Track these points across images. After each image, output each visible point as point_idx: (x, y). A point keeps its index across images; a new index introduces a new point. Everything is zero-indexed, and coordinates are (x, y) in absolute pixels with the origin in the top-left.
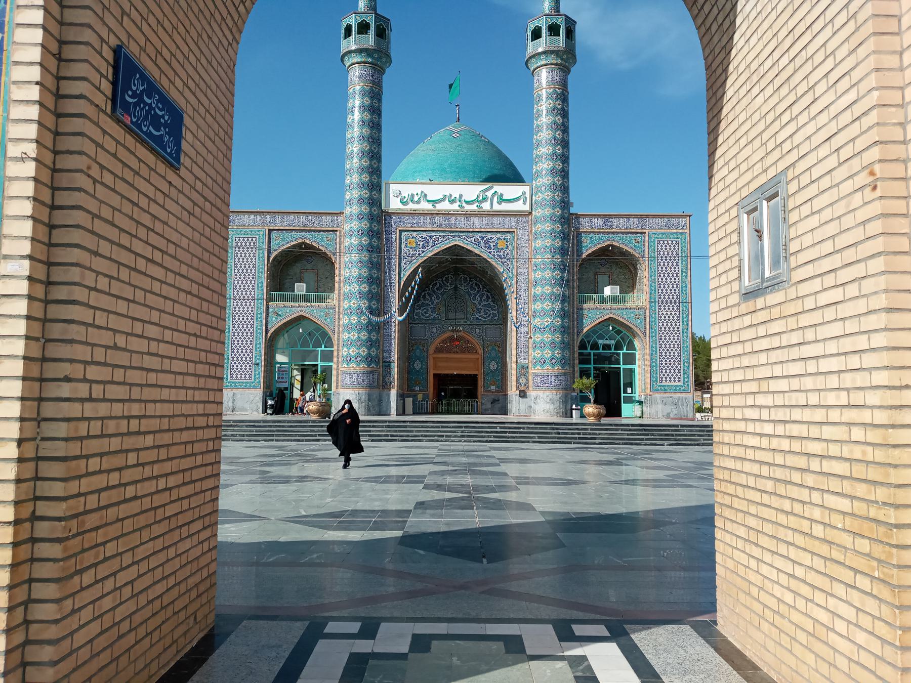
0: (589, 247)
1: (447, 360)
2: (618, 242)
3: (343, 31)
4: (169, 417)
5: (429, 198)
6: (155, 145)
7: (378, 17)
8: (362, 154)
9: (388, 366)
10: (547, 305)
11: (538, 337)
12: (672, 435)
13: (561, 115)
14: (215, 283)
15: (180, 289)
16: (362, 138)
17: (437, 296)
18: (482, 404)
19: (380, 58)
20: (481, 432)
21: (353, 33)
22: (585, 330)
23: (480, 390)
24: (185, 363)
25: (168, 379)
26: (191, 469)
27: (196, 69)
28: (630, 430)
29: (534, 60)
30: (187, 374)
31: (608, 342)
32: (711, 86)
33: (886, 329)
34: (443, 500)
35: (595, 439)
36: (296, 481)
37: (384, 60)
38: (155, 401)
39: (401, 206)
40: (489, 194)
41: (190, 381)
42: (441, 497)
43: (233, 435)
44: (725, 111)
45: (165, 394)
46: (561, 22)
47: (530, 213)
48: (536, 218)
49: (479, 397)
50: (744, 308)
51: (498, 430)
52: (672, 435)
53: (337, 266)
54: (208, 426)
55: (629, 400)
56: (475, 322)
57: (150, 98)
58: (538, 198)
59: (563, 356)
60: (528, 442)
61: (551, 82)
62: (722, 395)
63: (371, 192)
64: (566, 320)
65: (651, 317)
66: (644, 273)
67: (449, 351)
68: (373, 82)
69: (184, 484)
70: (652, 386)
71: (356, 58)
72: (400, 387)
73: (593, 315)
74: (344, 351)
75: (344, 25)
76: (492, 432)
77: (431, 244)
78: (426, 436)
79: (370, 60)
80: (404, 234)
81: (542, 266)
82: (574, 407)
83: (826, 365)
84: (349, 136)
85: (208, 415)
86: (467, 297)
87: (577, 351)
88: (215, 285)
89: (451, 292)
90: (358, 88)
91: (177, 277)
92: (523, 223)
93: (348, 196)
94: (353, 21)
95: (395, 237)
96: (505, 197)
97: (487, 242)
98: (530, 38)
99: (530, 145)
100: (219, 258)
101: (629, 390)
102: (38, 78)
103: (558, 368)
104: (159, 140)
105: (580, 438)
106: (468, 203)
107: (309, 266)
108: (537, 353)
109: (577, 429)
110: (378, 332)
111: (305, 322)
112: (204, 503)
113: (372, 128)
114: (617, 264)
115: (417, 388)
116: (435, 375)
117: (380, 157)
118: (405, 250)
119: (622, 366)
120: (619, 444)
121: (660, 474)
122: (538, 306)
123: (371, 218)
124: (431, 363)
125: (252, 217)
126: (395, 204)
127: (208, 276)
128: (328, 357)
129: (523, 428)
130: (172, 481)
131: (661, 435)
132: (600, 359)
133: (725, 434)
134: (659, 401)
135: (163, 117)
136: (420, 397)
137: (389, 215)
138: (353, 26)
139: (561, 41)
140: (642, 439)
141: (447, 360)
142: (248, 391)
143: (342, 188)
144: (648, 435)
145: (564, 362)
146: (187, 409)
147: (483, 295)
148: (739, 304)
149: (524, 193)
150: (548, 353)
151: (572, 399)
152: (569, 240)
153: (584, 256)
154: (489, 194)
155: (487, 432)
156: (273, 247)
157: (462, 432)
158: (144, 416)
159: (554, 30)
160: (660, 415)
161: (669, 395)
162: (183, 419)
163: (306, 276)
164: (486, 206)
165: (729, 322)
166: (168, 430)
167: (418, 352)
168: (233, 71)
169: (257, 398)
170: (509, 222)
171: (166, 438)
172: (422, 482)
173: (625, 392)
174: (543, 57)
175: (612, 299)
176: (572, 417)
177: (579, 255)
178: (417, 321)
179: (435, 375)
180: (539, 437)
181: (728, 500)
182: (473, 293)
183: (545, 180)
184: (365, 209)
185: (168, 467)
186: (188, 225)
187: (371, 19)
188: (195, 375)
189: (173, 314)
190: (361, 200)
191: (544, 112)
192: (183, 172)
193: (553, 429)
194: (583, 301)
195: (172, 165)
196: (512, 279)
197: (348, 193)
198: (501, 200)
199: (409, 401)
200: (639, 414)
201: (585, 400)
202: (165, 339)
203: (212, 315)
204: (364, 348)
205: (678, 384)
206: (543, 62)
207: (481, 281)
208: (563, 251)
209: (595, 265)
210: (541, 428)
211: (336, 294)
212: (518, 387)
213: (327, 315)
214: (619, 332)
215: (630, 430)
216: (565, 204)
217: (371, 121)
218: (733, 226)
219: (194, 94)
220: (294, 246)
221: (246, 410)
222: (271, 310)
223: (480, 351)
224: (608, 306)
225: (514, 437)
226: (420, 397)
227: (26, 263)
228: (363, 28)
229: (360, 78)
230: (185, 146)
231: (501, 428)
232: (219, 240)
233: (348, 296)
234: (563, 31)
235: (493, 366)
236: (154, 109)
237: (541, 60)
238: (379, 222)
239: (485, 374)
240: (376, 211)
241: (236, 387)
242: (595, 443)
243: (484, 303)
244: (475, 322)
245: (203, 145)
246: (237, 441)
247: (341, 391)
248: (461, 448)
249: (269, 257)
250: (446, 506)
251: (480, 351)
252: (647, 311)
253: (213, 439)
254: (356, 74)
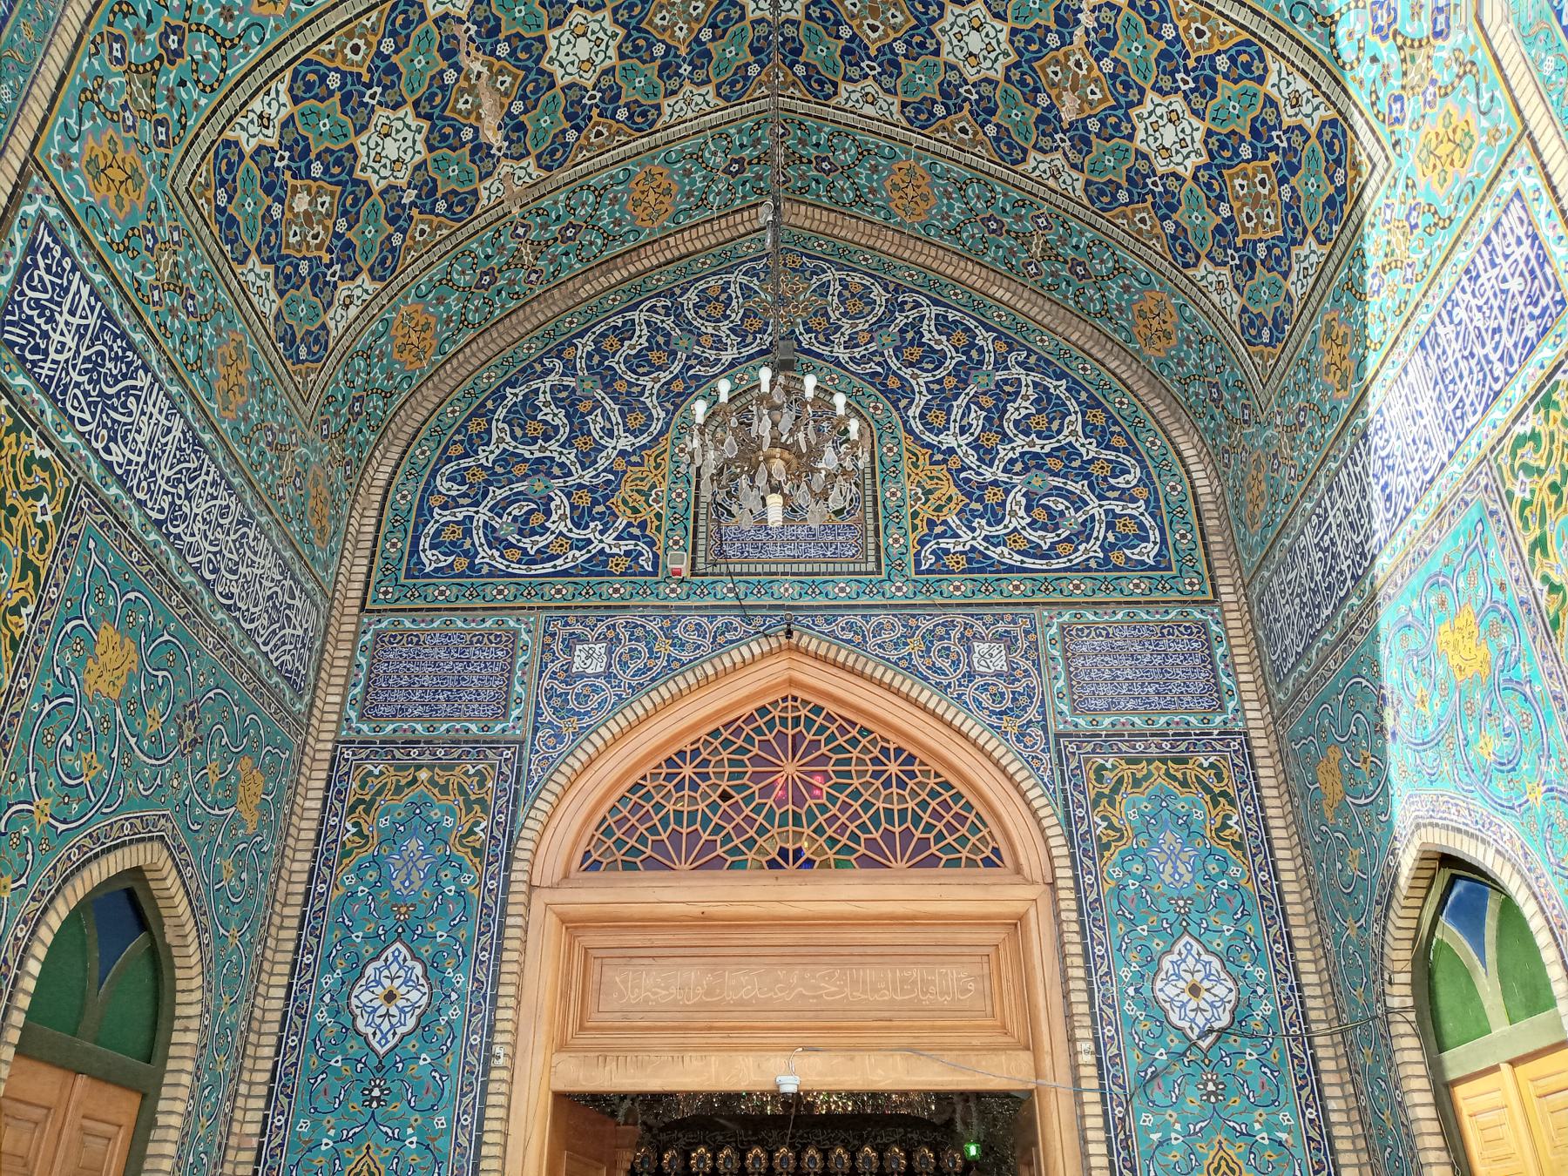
1: (712, 934)
17: (630, 403)
56: (957, 587)
124: (536, 966)
141: (712, 934)
147: (1004, 394)
182: (920, 381)
207: (978, 304)
239: (1121, 1094)
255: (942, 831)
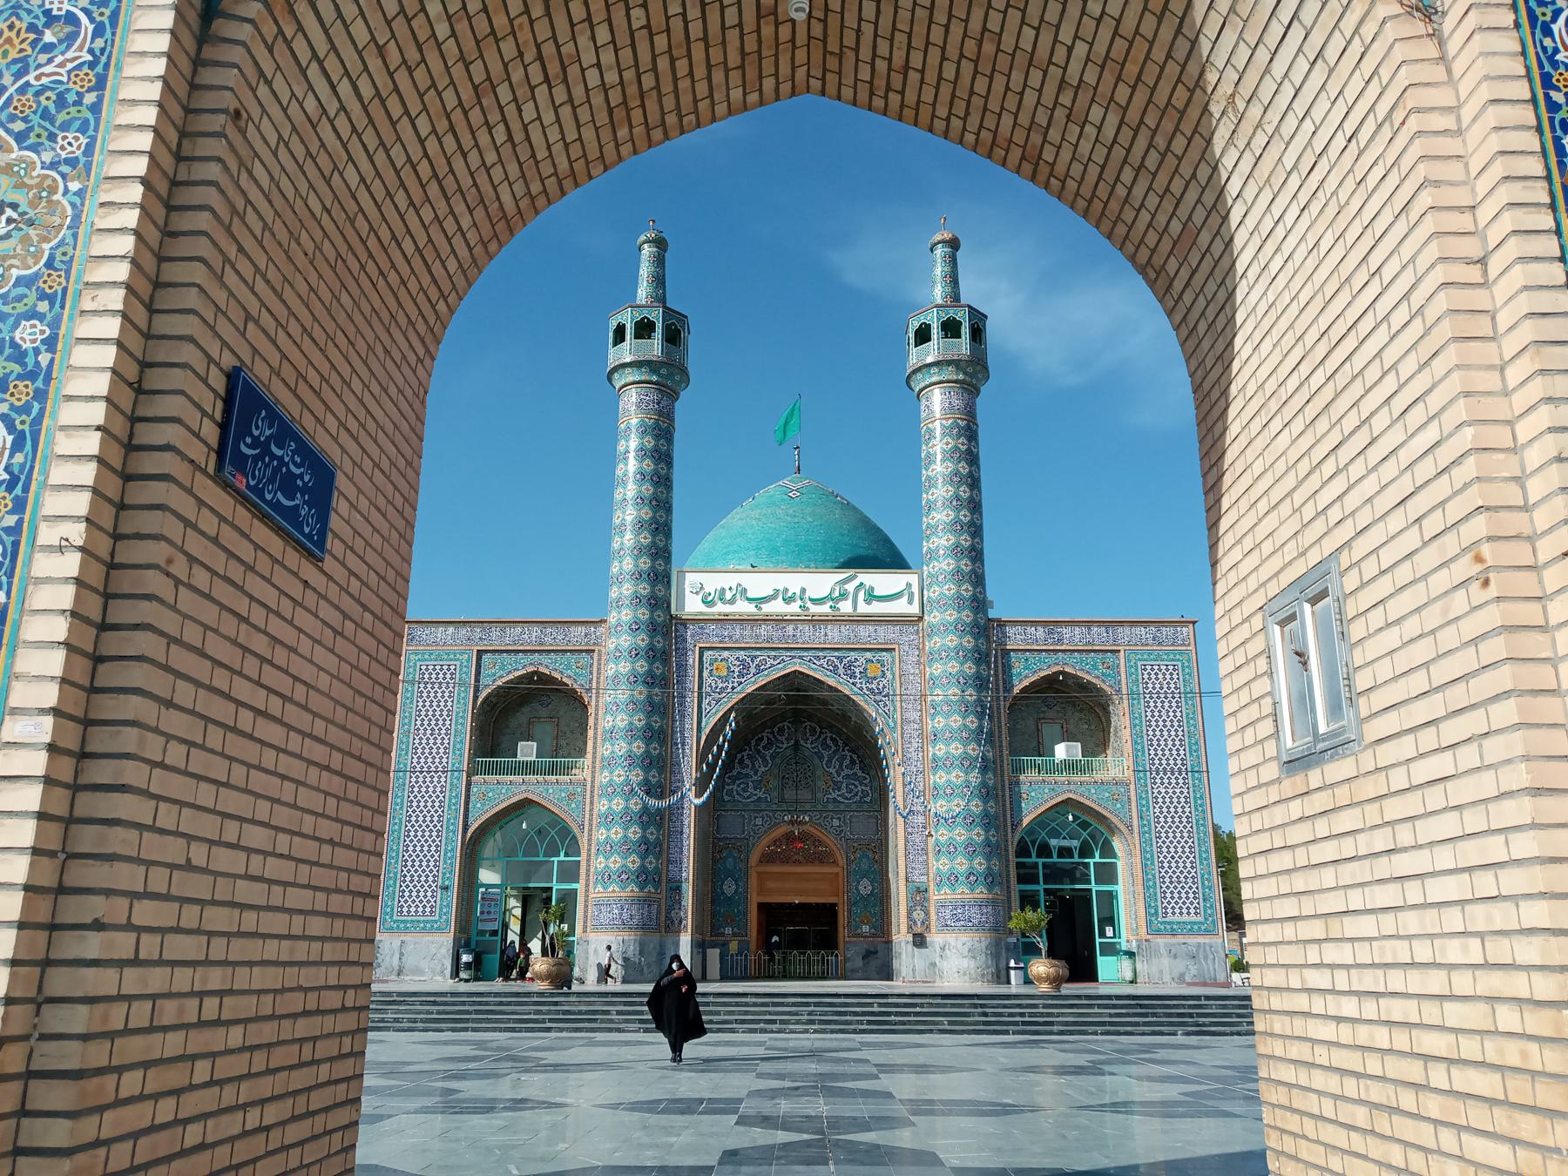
0: (1024, 675)
2: (1073, 666)
3: (611, 334)
4: (275, 991)
5: (750, 595)
6: (285, 522)
7: (668, 312)
8: (640, 525)
9: (676, 889)
10: (957, 777)
11: (942, 835)
12: (1191, 1015)
13: (966, 460)
14: (373, 749)
15: (310, 762)
16: (641, 500)
17: (764, 760)
18: (846, 960)
19: (670, 376)
20: (845, 1014)
21: (628, 337)
22: (1026, 821)
23: (843, 933)
24: (311, 892)
25: (276, 923)
26: (309, 1089)
27: (361, 401)
28: (1115, 1006)
29: (919, 376)
30: (313, 912)
31: (1065, 843)
32: (1204, 418)
33: (1534, 826)
34: (773, 1147)
35: (1052, 1024)
36: (505, 1109)
37: (677, 378)
38: (251, 964)
39: (703, 608)
40: (851, 587)
41: (317, 926)
42: (770, 1142)
43: (396, 1020)
44: (1229, 457)
45: (271, 950)
46: (962, 316)
47: (921, 618)
48: (931, 626)
49: (841, 945)
50: (1290, 786)
51: (876, 1009)
52: (1191, 1015)
53: (591, 710)
54: (344, 1009)
55: (1111, 950)
57: (281, 447)
58: (932, 593)
59: (989, 868)
60: (931, 1031)
61: (949, 410)
62: (1265, 944)
63: (653, 587)
64: (991, 803)
65: (1139, 798)
66: (1121, 720)
67: (785, 859)
68: (660, 413)
69: (294, 1118)
70: (1149, 924)
71: (631, 376)
72: (697, 929)
73: (1037, 794)
74: (599, 863)
75: (613, 324)
76: (864, 1014)
77: (753, 670)
78: (743, 1022)
79: (654, 378)
80: (707, 654)
81: (945, 708)
82: (1012, 964)
83: (1440, 889)
84: (618, 497)
85: (345, 988)
86: (816, 761)
87: (1013, 860)
88: (372, 754)
89: (789, 752)
90: (634, 421)
91: (307, 740)
92: (909, 635)
93: (614, 593)
94: (628, 319)
95: (693, 659)
96: (876, 593)
97: (849, 667)
98: (912, 341)
99: (915, 509)
100: (381, 706)
101: (1109, 931)
102: (100, 420)
103: (981, 892)
104: (291, 514)
105: (1024, 1023)
106: (815, 601)
107: (543, 712)
108: (940, 865)
109: (1019, 1006)
110: (660, 826)
111: (534, 810)
112: (329, 1156)
113: (656, 484)
114: (1073, 705)
115: (728, 930)
116: (761, 906)
117: (670, 530)
118: (708, 680)
119: (1094, 887)
120: (1095, 1033)
121: (1173, 1092)
122: (940, 778)
123: (653, 628)
124: (753, 882)
125: (451, 630)
126: (692, 605)
127: (362, 738)
128: (570, 873)
129: (922, 1005)
130: (272, 1114)
131: (1170, 1015)
132: (1054, 874)
133: (1275, 1017)
134: (1163, 950)
135: (301, 476)
136: (733, 946)
137: (684, 623)
138: (628, 326)
139: (963, 345)
140: (1137, 1024)
142: (429, 938)
143: (605, 581)
144: (1145, 1015)
145: (991, 879)
146: (308, 977)
147: (844, 758)
148: (1278, 781)
149: (909, 585)
150: (961, 864)
151: (1008, 950)
152: (988, 664)
153: (1016, 690)
154: (851, 587)
155: (856, 1014)
156: (483, 681)
157: (810, 1014)
158: (231, 992)
159: (951, 329)
160: (1167, 978)
161: (1180, 939)
162: (300, 995)
163: (538, 729)
164: (846, 607)
165: (1265, 812)
166: (272, 1017)
167: (730, 862)
168: (423, 403)
169: (443, 951)
170: (884, 634)
171: (267, 1032)
172: (735, 1111)
173: (1102, 935)
174: (934, 370)
175: (1069, 766)
176: (1009, 982)
177: (1008, 689)
178: (729, 806)
179: (761, 906)
180: (950, 1023)
181: (1288, 1144)
182: (826, 753)
183: (945, 564)
184: (643, 614)
185: (265, 1087)
186: (332, 651)
187: (656, 316)
188: (326, 914)
189: (295, 806)
190: (637, 599)
191: (939, 457)
192: (329, 564)
193: (975, 1006)
194: (1018, 769)
195: (311, 554)
196: (894, 729)
197: (615, 588)
198: (871, 597)
199: (714, 954)
200: (1129, 975)
201: (1031, 950)
202: (278, 851)
203: (364, 806)
204: (634, 857)
205: (1193, 918)
206: (934, 379)
207: (839, 733)
208: (980, 683)
209: (1036, 708)
210: (953, 1005)
211: (588, 760)
212: (910, 927)
213: (571, 796)
214: (1085, 825)
215: (1115, 1006)
216: (979, 603)
217: (656, 473)
218: (1257, 645)
219: (356, 439)
220: (520, 679)
221: (422, 973)
222: (474, 789)
223: (842, 861)
224: (1063, 778)
225: (904, 1023)
226: (733, 946)
227: (49, 721)
228: (644, 329)
229: (638, 406)
230: (335, 522)
231: (880, 1005)
232: (383, 676)
233: (609, 763)
234: (965, 330)
235: (865, 887)
236: (287, 465)
237: (931, 376)
238: (667, 635)
239: (851, 904)
240: (660, 617)
241: (407, 931)
242: (1051, 1033)
243: (846, 772)
244: (831, 807)
245: (366, 519)
246: (404, 1030)
247: (592, 936)
248: (807, 1044)
249: (476, 698)
250: (778, 1158)
251: (842, 861)
252: (1132, 787)
253: (353, 1033)
254: (631, 397)
255: (823, 858)
